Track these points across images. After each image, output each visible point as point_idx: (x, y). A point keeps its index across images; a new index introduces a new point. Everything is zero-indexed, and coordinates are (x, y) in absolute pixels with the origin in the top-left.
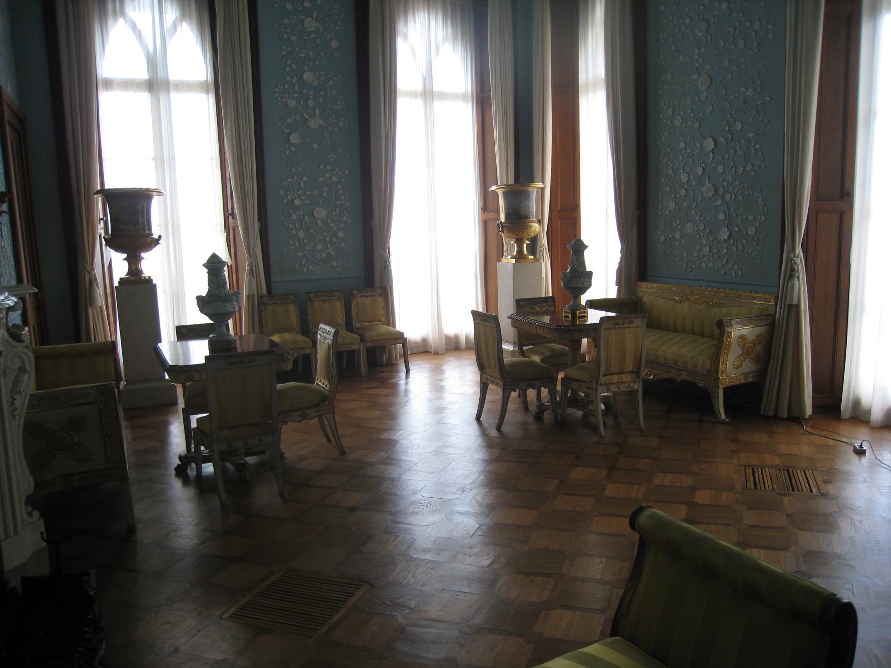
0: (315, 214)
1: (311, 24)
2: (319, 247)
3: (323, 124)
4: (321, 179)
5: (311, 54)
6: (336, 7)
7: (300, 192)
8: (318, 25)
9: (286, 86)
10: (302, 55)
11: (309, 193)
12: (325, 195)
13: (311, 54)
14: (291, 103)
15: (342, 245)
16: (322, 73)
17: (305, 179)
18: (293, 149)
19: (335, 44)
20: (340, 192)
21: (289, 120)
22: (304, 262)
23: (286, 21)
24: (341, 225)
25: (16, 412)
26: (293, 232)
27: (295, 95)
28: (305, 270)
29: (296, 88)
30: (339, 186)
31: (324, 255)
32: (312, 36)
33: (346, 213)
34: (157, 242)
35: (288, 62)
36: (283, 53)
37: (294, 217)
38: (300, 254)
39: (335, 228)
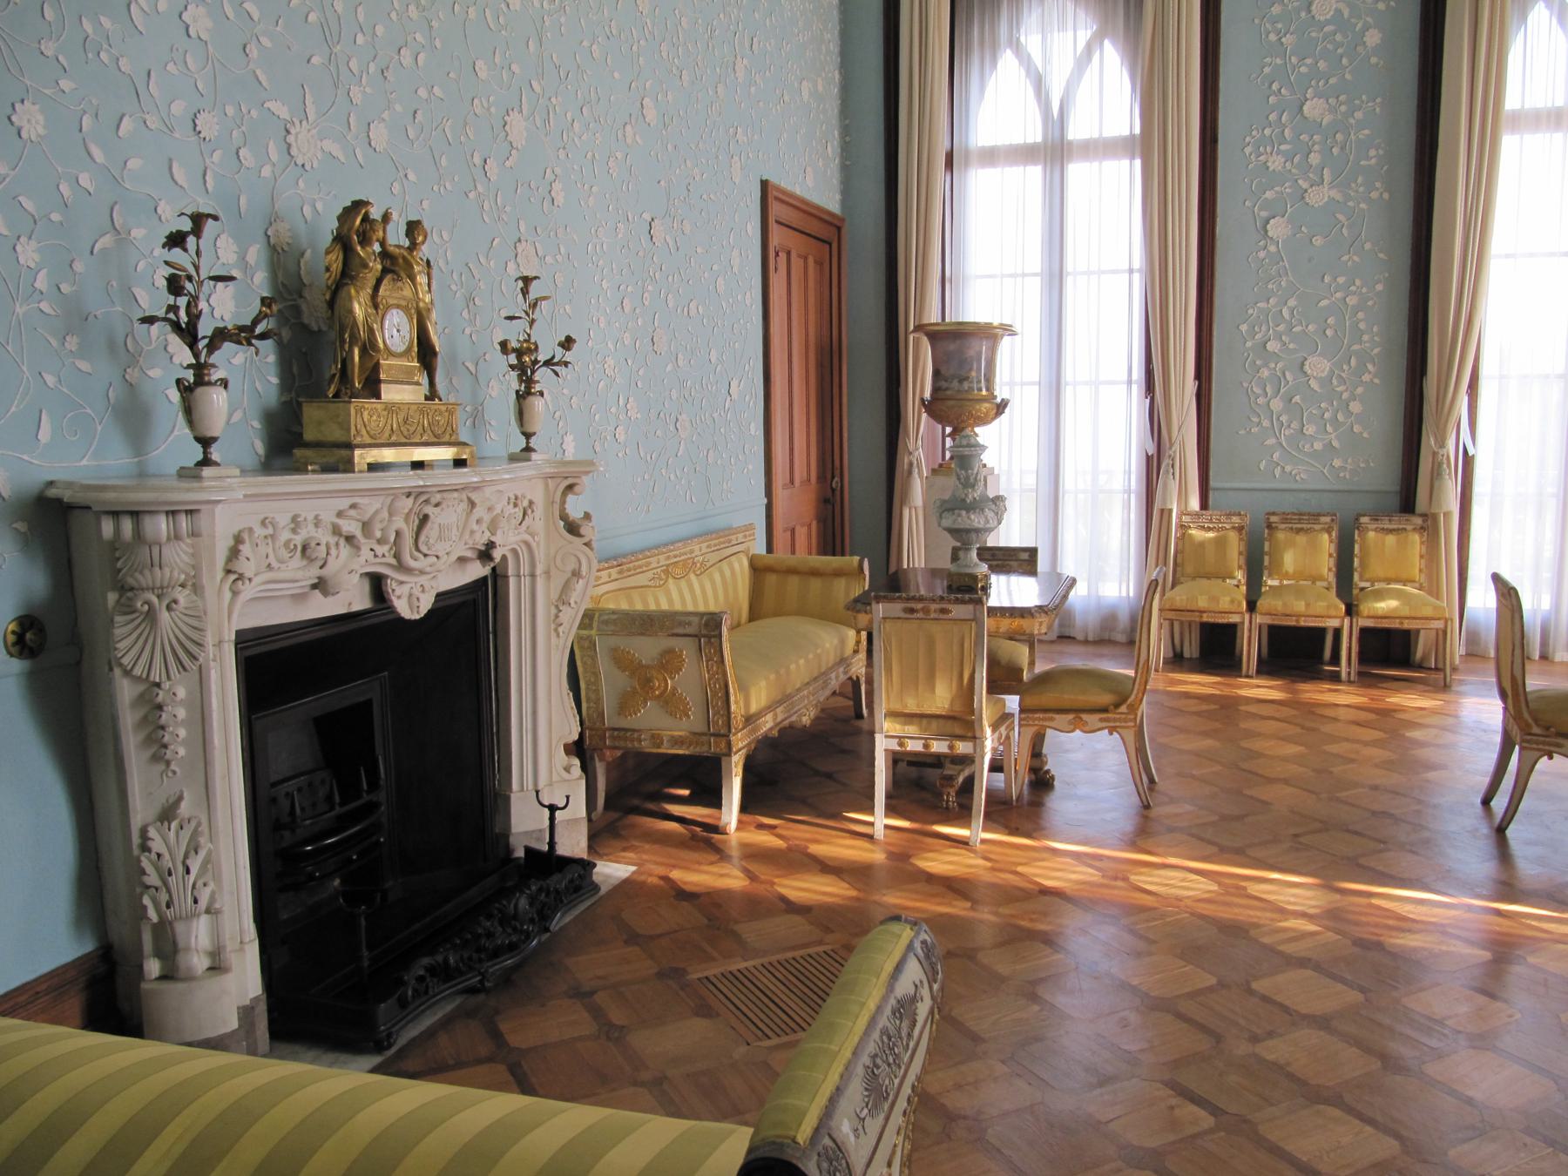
0: (1307, 368)
2: (1310, 430)
3: (1338, 197)
4: (1324, 303)
5: (1322, 65)
7: (1281, 328)
9: (1267, 132)
10: (1303, 69)
11: (1297, 329)
12: (1328, 332)
14: (1276, 163)
15: (1357, 428)
17: (1292, 303)
18: (1272, 248)
19: (1373, 38)
20: (1362, 326)
21: (1268, 194)
22: (1276, 456)
24: (1360, 390)
25: (561, 629)
26: (1261, 400)
27: (1283, 147)
28: (1278, 471)
30: (1361, 315)
31: (1318, 446)
32: (1328, 29)
33: (1370, 367)
34: (1001, 408)
35: (1275, 87)
36: (1267, 70)
37: (1265, 373)
38: (1271, 441)
39: (1345, 396)
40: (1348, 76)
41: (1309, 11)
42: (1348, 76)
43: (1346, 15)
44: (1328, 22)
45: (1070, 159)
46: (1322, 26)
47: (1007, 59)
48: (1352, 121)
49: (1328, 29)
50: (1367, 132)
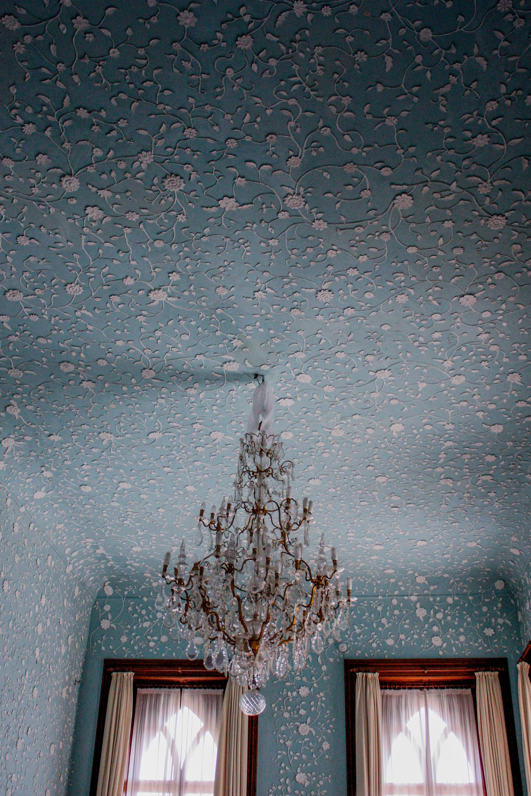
1: (304, 729)
5: (304, 756)
6: (328, 712)
8: (312, 729)
9: (280, 787)
13: (304, 756)
16: (313, 773)
19: (326, 746)
23: (283, 728)
29: (289, 788)
32: (306, 739)
35: (283, 765)
36: (279, 757)
40: (316, 763)
41: (298, 731)
42: (316, 763)
43: (314, 734)
44: (306, 736)
45: (185, 792)
46: (303, 738)
47: (159, 734)
48: (318, 785)
49: (306, 739)
50: (325, 791)
